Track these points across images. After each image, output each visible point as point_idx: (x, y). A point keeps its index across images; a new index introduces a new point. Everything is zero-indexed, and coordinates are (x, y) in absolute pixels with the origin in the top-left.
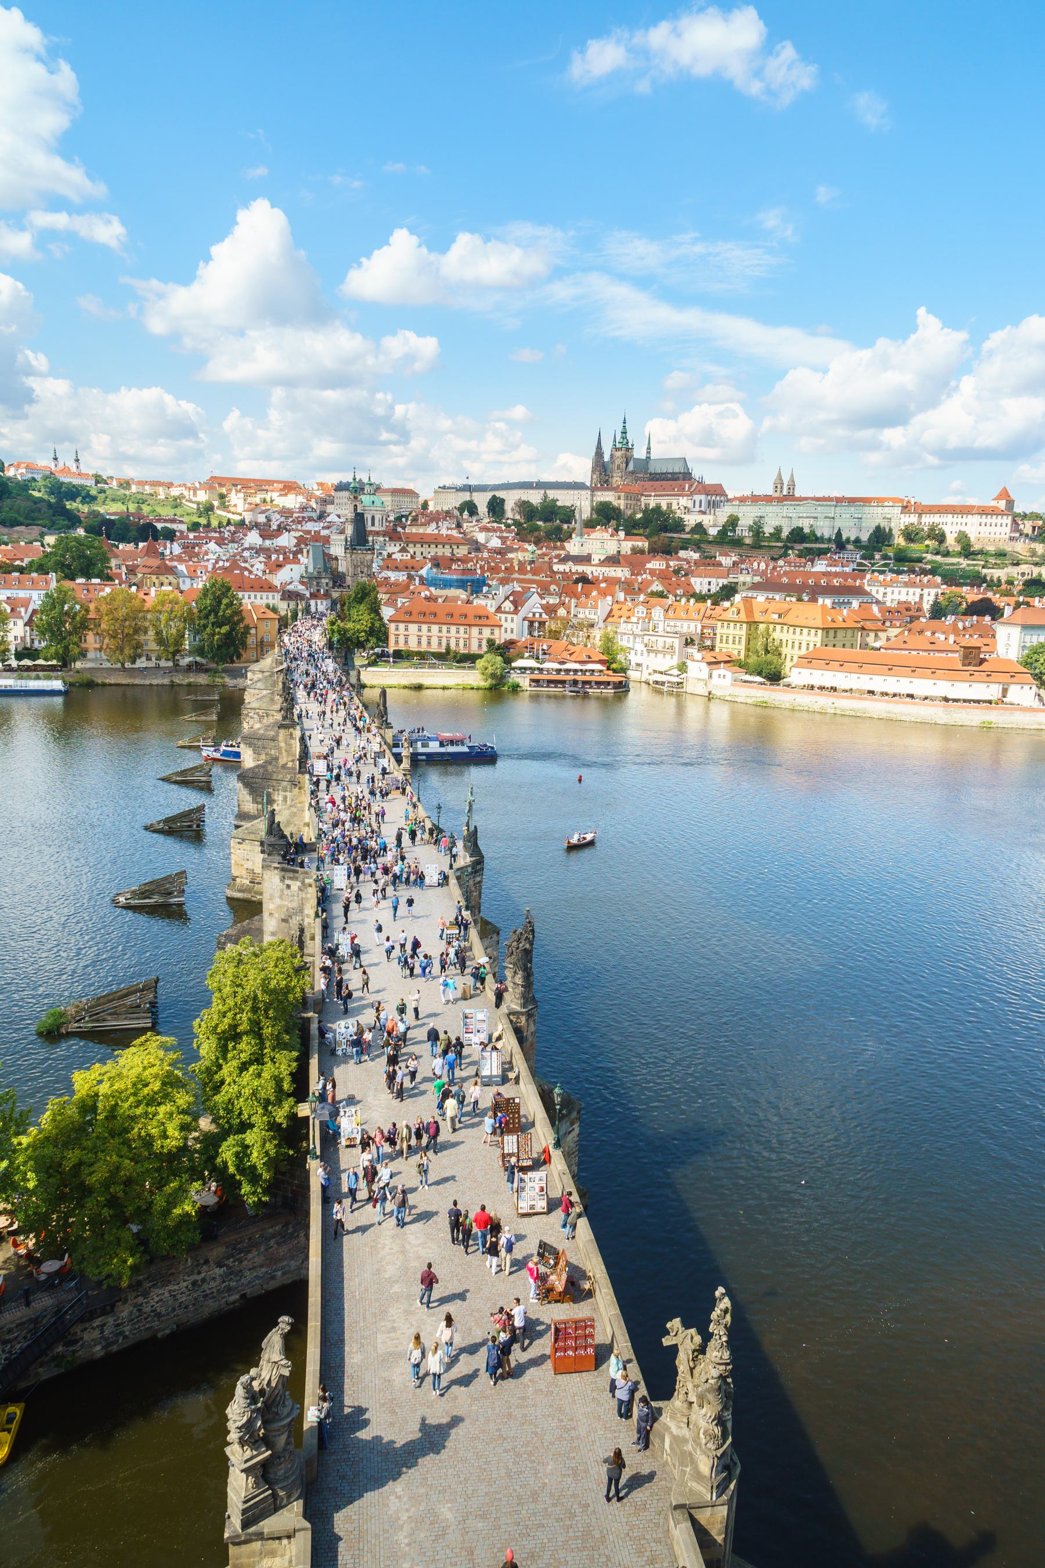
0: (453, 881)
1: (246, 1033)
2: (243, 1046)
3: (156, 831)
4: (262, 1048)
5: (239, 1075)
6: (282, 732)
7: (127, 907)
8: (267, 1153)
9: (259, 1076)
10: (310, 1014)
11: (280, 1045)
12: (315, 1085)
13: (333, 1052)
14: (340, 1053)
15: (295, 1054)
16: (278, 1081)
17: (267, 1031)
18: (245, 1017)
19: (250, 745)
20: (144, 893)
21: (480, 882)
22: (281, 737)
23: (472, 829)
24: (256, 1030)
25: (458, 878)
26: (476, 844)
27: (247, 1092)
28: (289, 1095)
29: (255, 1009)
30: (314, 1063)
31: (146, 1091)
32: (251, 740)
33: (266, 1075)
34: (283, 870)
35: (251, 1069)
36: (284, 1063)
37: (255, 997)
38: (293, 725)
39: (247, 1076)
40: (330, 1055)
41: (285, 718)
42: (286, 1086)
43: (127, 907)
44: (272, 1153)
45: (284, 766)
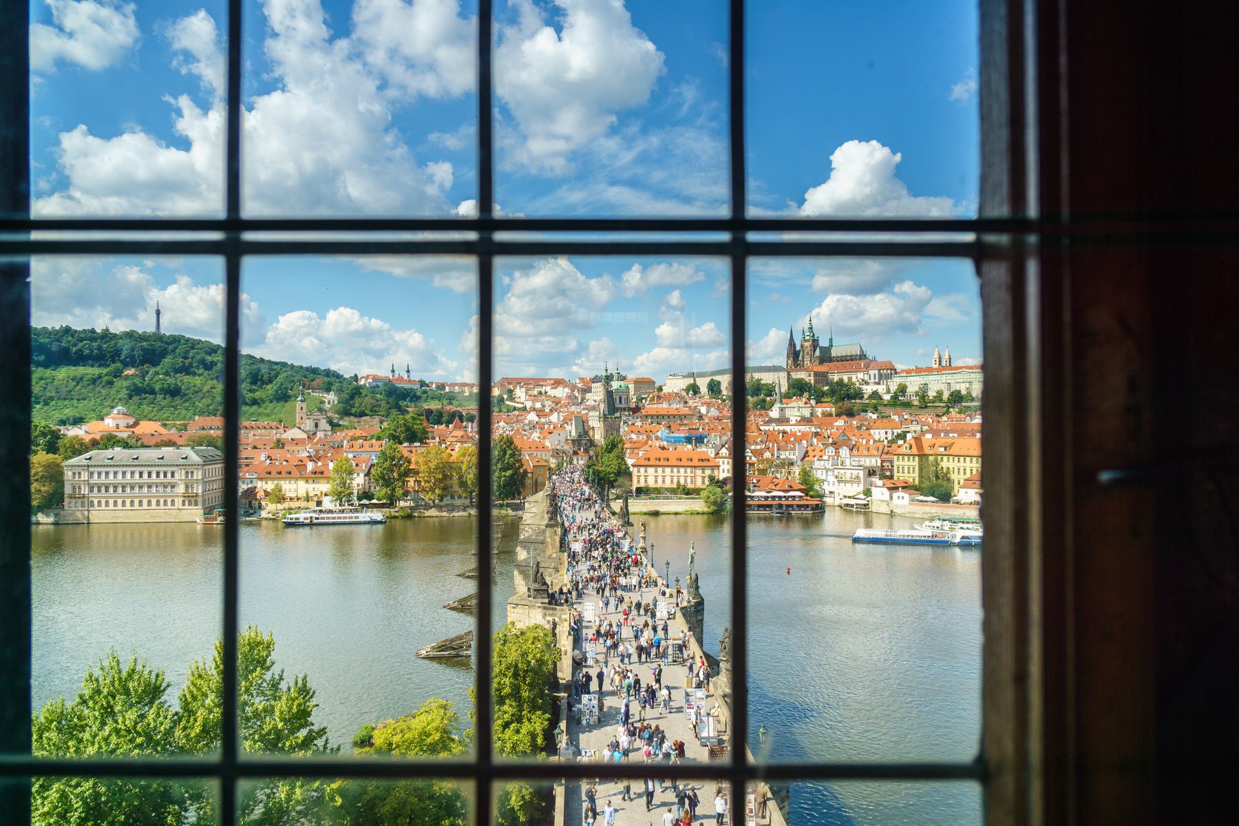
0: (679, 615)
1: (508, 696)
2: (506, 708)
3: (453, 609)
4: (521, 710)
5: (503, 732)
6: (548, 530)
7: (427, 658)
8: (523, 797)
9: (518, 732)
10: (562, 694)
11: (534, 708)
12: (563, 741)
13: (579, 722)
14: (584, 722)
15: (547, 716)
16: (533, 736)
17: (525, 694)
18: (507, 681)
19: (525, 548)
20: (442, 648)
21: (702, 620)
22: (548, 534)
23: (694, 577)
24: (516, 694)
25: (684, 615)
26: (697, 588)
27: (509, 745)
28: (542, 750)
29: (515, 675)
30: (563, 725)
31: (429, 740)
32: (526, 544)
33: (523, 731)
34: (545, 608)
35: (512, 726)
36: (537, 723)
37: (516, 666)
38: (556, 525)
39: (509, 732)
40: (575, 725)
41: (551, 519)
42: (539, 741)
43: (427, 658)
44: (527, 797)
45: (550, 557)
